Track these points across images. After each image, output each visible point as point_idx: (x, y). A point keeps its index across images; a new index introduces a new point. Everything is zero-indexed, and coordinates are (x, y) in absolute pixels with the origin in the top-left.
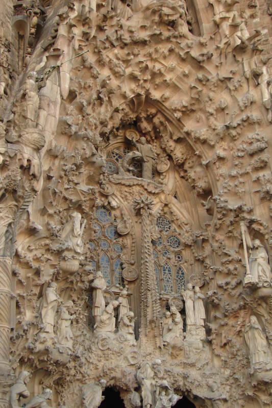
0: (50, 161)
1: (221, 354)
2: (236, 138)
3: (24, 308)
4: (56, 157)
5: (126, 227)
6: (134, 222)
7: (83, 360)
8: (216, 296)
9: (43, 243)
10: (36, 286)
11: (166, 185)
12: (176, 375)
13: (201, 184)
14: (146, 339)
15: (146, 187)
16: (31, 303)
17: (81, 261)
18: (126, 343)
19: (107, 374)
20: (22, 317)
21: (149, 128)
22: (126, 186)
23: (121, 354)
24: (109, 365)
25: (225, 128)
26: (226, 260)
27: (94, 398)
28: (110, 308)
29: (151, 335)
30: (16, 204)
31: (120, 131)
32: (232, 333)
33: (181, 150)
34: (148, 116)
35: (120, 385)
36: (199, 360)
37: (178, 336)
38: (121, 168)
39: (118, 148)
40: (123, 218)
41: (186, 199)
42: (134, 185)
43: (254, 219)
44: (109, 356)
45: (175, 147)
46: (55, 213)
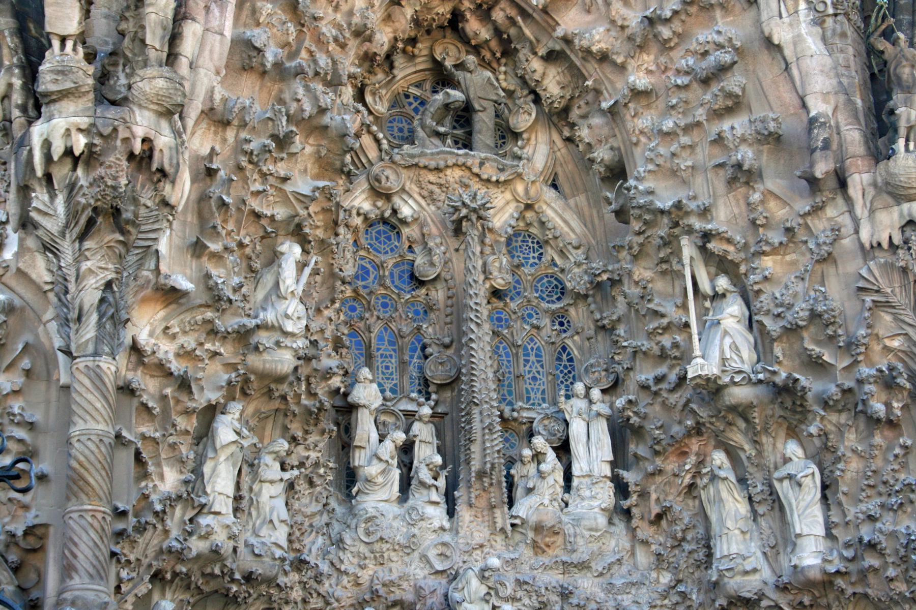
0: (216, 133)
1: (650, 540)
2: (672, 44)
3: (159, 465)
4: (228, 123)
5: (432, 264)
6: (452, 250)
7: (325, 567)
8: (635, 410)
9: (199, 318)
10: (187, 412)
11: (528, 160)
13: (602, 154)
15: (476, 170)
16: (177, 453)
17: (296, 351)
19: (379, 597)
20: (151, 485)
21: (485, 34)
22: (430, 170)
23: (413, 550)
25: (646, 22)
26: (656, 324)
28: (388, 449)
29: (482, 503)
30: (121, 238)
32: (674, 491)
33: (558, 78)
36: (601, 554)
37: (546, 502)
38: (419, 129)
39: (418, 85)
40: (427, 244)
41: (577, 190)
43: (711, 230)
44: (385, 555)
45: (544, 74)
46: (226, 249)
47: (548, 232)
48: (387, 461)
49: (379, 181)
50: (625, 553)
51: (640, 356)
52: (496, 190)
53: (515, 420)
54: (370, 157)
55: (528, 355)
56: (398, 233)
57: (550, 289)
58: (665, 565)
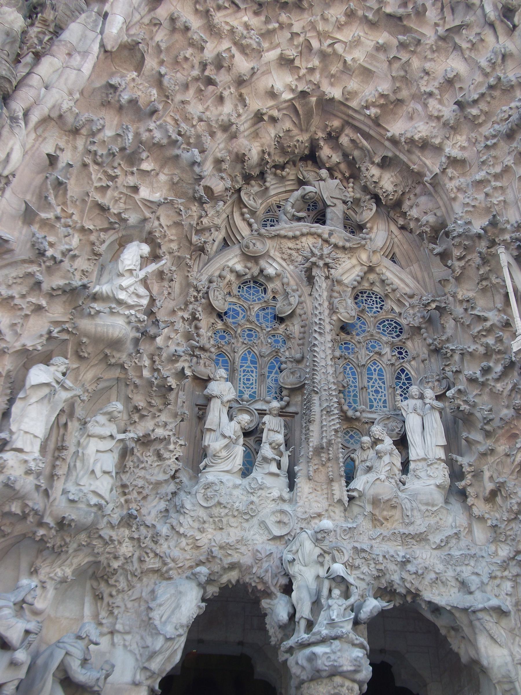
1: (487, 516)
5: (290, 304)
6: (306, 295)
7: (164, 530)
12: (381, 559)
14: (311, 484)
18: (263, 493)
19: (214, 557)
21: (336, 158)
24: (220, 538)
27: (178, 606)
29: (321, 477)
31: (287, 170)
32: (507, 471)
33: (391, 179)
34: (329, 134)
35: (252, 581)
37: (383, 477)
41: (411, 261)
42: (303, 235)
45: (381, 177)
47: (387, 288)
48: (230, 437)
49: (247, 247)
50: (462, 529)
51: (467, 357)
52: (343, 256)
53: (357, 419)
54: (244, 235)
55: (372, 374)
56: (265, 289)
57: (390, 329)
58: (502, 538)
